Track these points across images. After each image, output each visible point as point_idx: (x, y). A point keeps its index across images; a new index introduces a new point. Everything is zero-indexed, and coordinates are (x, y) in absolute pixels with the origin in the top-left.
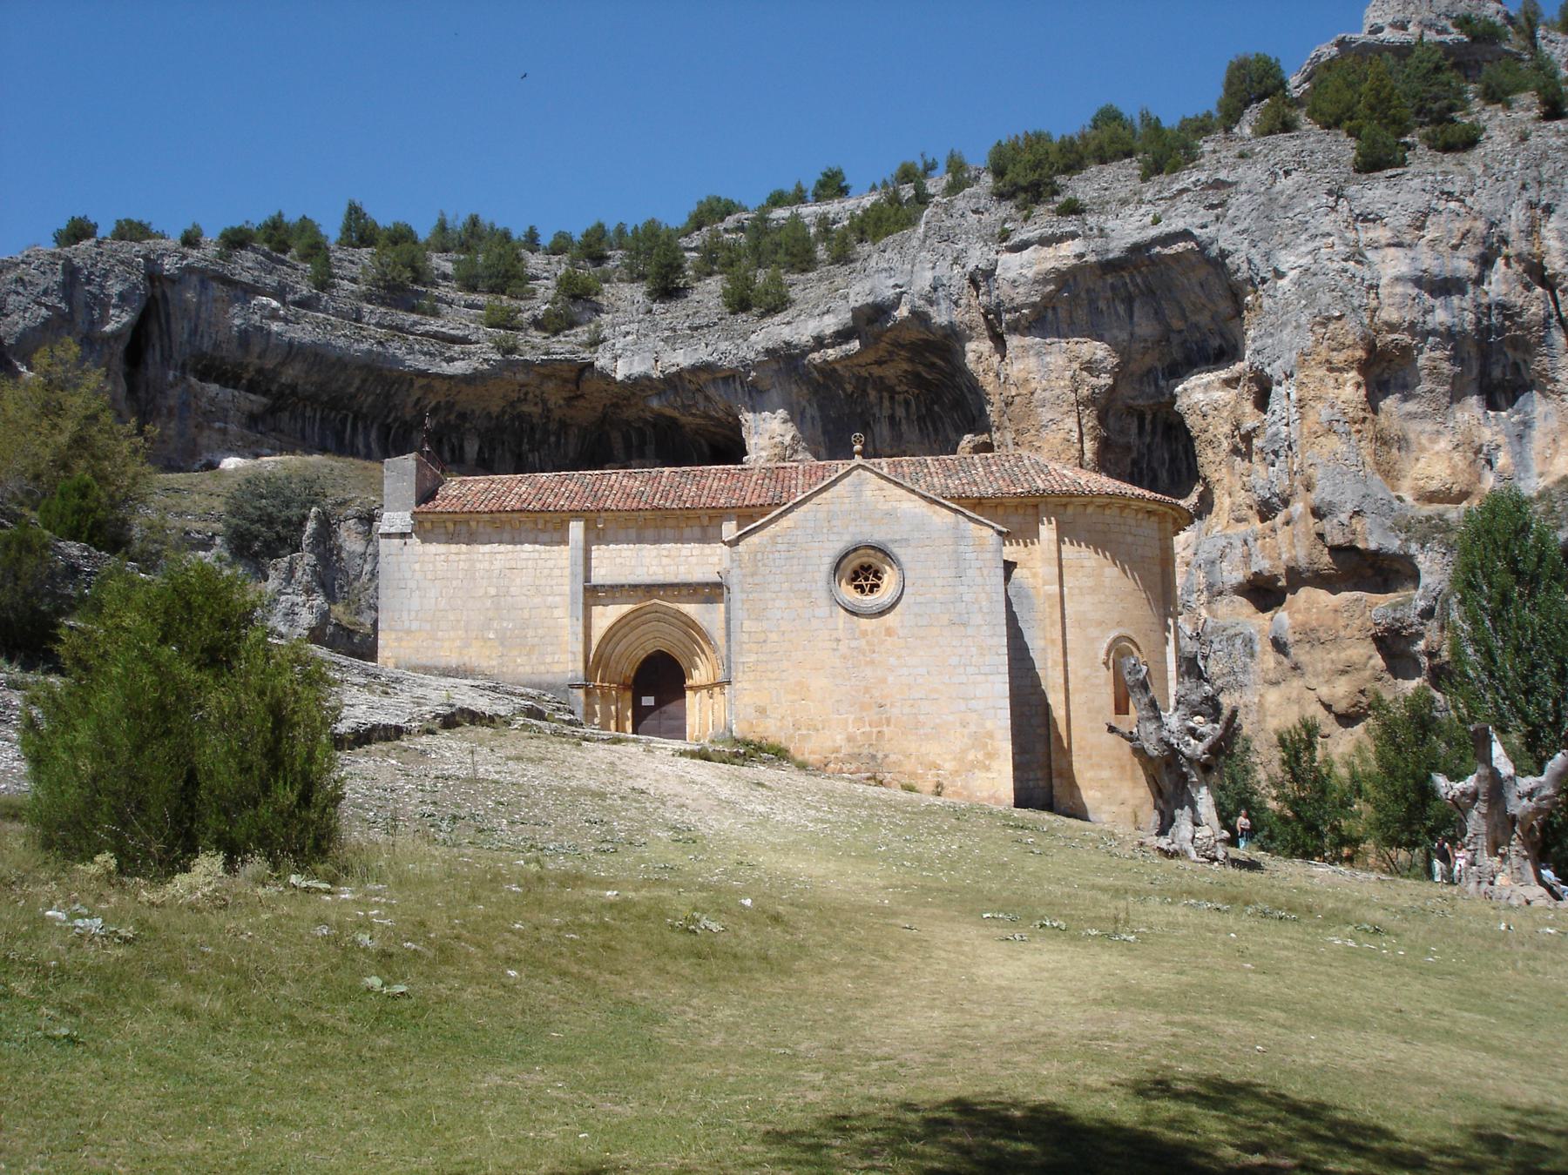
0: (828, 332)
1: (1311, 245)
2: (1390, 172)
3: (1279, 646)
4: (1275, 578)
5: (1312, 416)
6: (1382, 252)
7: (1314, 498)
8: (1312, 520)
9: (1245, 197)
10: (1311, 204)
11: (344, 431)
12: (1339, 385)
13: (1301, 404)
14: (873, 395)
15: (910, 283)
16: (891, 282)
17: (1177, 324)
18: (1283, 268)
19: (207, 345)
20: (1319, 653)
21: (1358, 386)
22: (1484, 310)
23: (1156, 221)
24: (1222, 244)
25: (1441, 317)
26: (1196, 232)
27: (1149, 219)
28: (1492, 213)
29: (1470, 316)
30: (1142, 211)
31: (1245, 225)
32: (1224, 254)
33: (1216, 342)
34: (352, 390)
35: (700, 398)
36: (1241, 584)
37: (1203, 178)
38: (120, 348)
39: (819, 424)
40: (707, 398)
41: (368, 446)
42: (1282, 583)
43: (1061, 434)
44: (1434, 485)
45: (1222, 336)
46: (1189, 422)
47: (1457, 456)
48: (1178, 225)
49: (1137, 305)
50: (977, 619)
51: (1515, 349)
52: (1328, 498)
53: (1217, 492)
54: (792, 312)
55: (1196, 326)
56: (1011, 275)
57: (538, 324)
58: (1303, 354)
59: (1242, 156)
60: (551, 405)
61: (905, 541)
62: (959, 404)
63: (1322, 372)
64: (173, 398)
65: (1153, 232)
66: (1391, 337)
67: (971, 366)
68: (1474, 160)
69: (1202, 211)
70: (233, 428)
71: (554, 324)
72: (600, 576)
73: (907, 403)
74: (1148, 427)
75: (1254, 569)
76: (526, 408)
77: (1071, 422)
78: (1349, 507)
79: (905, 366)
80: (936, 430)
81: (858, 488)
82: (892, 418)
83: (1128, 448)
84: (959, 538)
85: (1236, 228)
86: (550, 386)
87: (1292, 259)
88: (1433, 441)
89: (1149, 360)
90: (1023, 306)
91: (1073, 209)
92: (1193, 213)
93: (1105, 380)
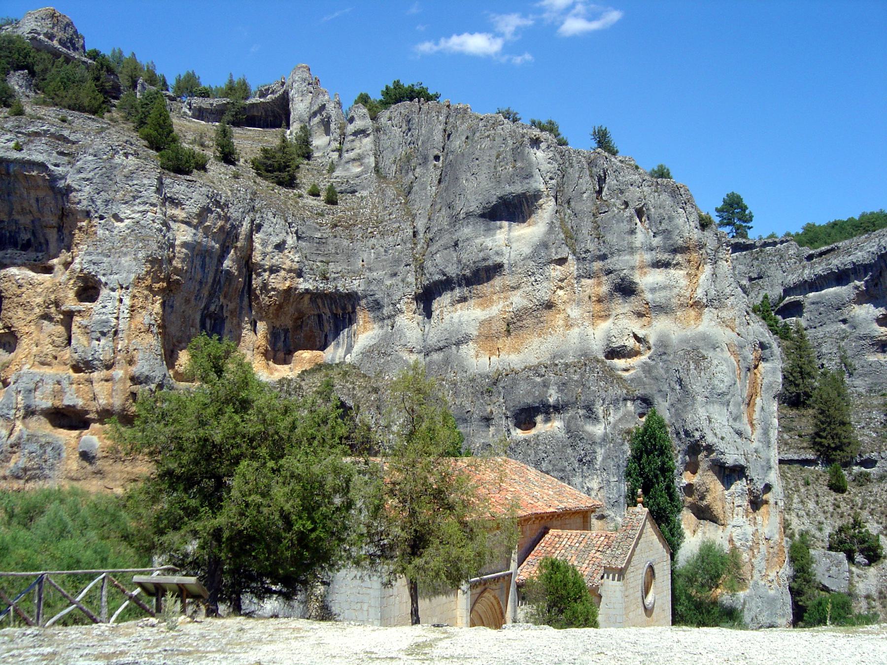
1: (142, 208)
3: (86, 456)
4: (87, 412)
5: (138, 319)
6: (178, 224)
7: (134, 370)
8: (129, 383)
9: (91, 158)
10: (146, 181)
13: (132, 309)
18: (122, 216)
20: (119, 466)
24: (69, 181)
27: (12, 144)
28: (235, 220)
30: (8, 137)
31: (90, 176)
32: (69, 189)
33: (25, 236)
36: (48, 409)
37: (53, 130)
42: (92, 416)
45: (34, 234)
51: (225, 297)
52: (147, 373)
55: (16, 222)
58: (138, 278)
63: (146, 292)
65: (16, 155)
66: (176, 277)
69: (55, 154)
75: (67, 402)
85: (82, 175)
87: (129, 212)
92: (50, 154)
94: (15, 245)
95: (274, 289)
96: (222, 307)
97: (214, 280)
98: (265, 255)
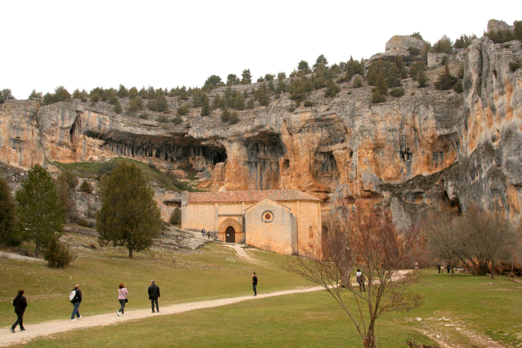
0: (249, 130)
1: (362, 120)
2: (381, 103)
12: (368, 153)
13: (359, 157)
14: (260, 145)
15: (270, 121)
16: (265, 120)
17: (333, 133)
19: (90, 128)
21: (372, 153)
22: (401, 137)
23: (328, 110)
25: (391, 138)
26: (337, 113)
29: (398, 137)
33: (342, 138)
34: (125, 139)
35: (215, 142)
38: (69, 130)
39: (246, 151)
40: (217, 143)
41: (128, 152)
43: (305, 159)
44: (389, 176)
46: (335, 157)
47: (394, 170)
48: (333, 111)
49: (323, 128)
50: (286, 223)
53: (341, 174)
54: (239, 123)
56: (294, 120)
57: (173, 121)
59: (349, 94)
60: (176, 142)
61: (274, 210)
62: (281, 147)
64: (81, 143)
67: (284, 141)
68: (403, 98)
70: (97, 149)
71: (177, 122)
72: (221, 213)
73: (268, 146)
74: (326, 157)
76: (169, 143)
77: (308, 156)
78: (369, 182)
79: (268, 139)
80: (275, 153)
81: (266, 202)
82: (264, 150)
83: (321, 162)
84: (283, 210)
86: (176, 137)
88: (389, 166)
89: (326, 142)
90: (297, 127)
91: (308, 105)
92: (337, 109)
93: (316, 146)
94: (339, 142)
95: (427, 137)
96: (408, 149)
97: (400, 139)
98: (420, 124)
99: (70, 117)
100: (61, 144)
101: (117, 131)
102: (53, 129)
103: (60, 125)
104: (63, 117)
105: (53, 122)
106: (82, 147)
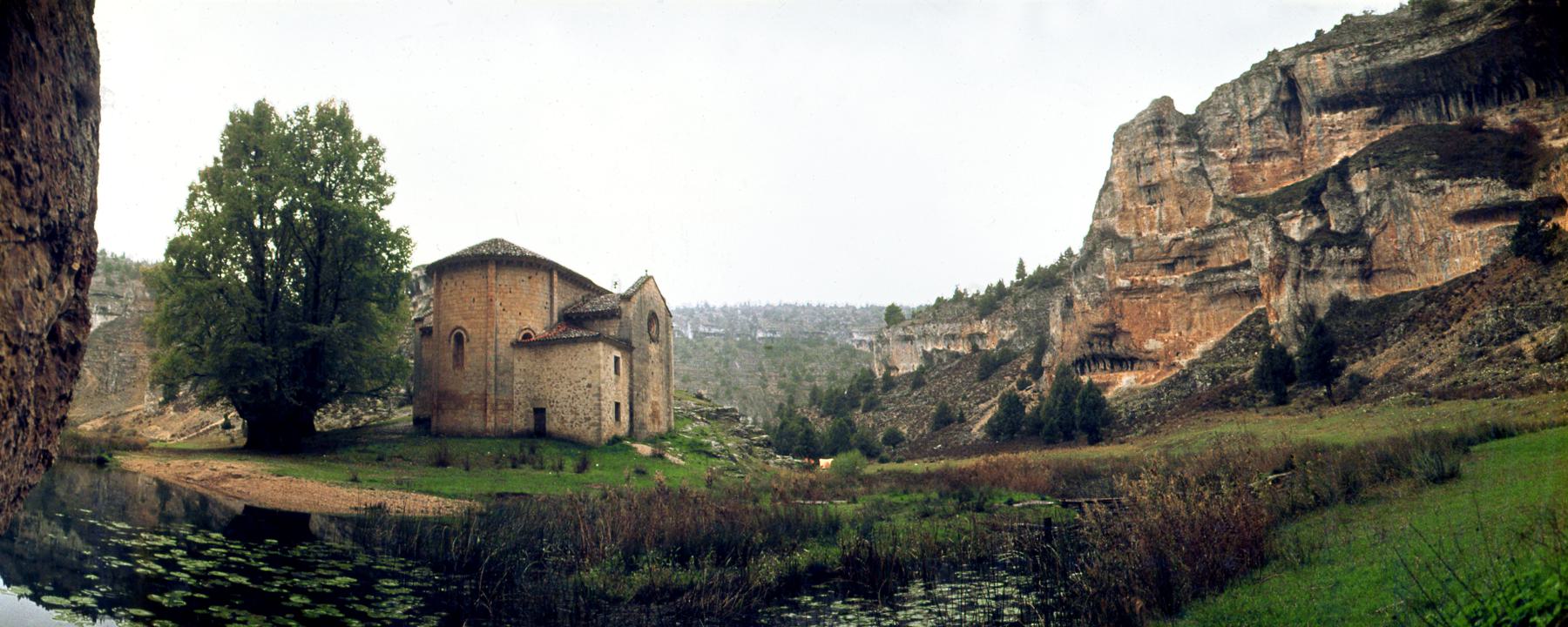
11: (1439, 107)
99: (1262, 90)
100: (1262, 155)
101: (1386, 72)
102: (1230, 131)
103: (1246, 116)
104: (1247, 98)
105: (1225, 118)
106: (1312, 143)
